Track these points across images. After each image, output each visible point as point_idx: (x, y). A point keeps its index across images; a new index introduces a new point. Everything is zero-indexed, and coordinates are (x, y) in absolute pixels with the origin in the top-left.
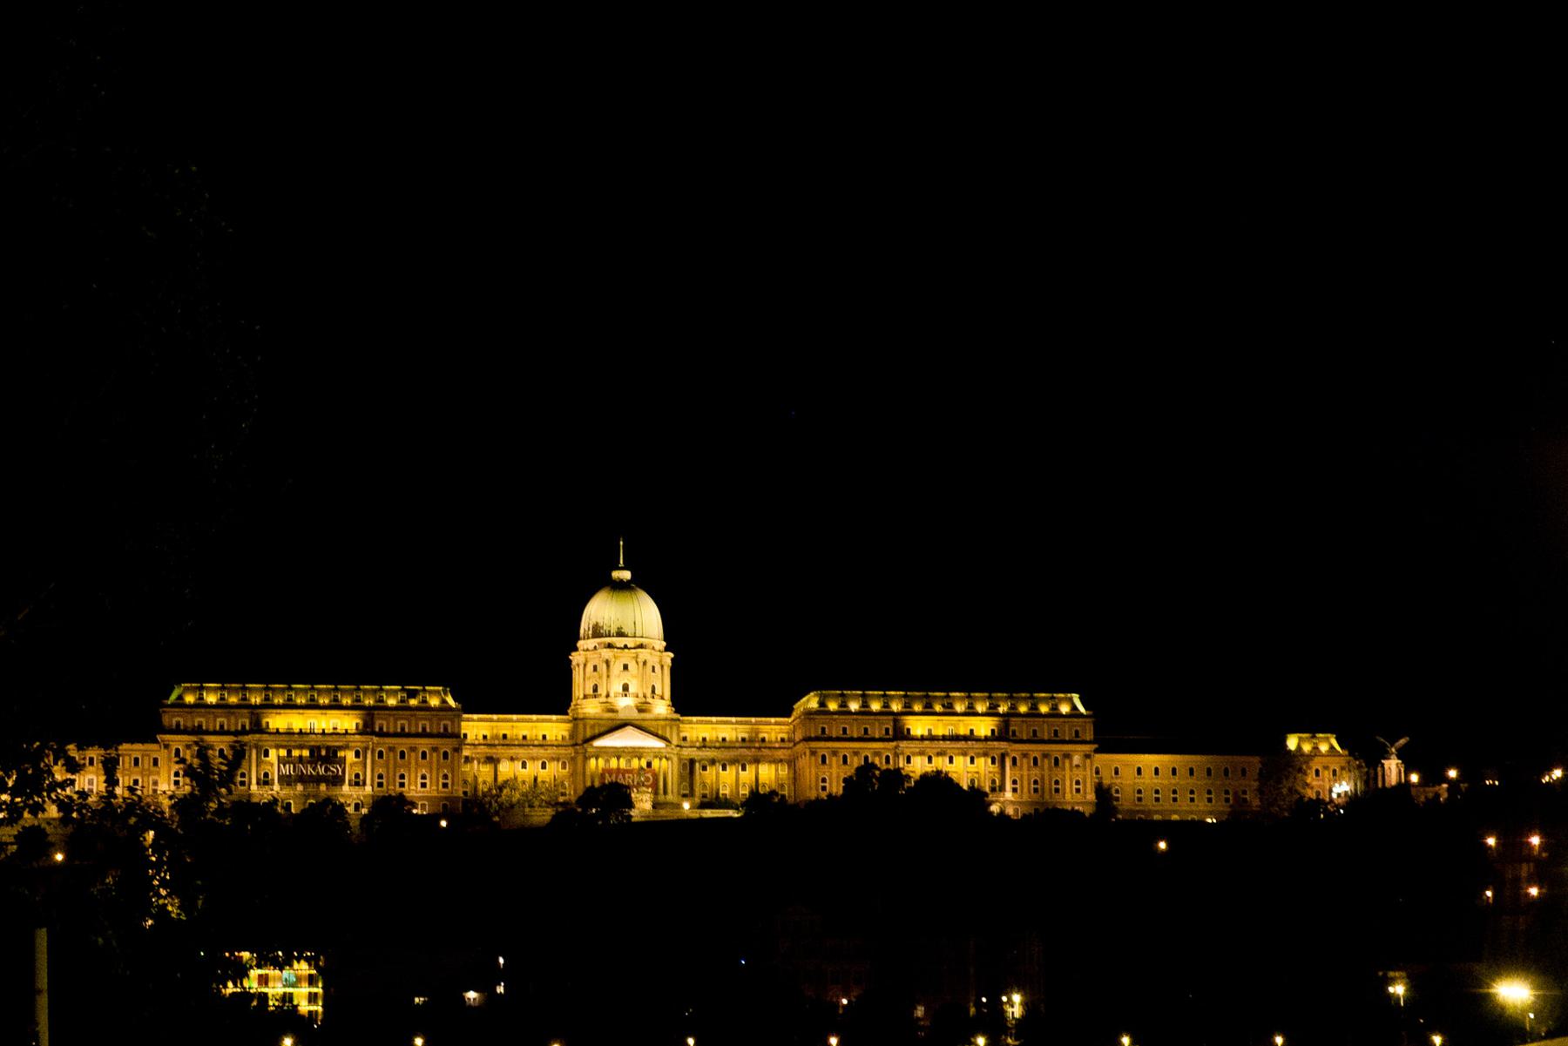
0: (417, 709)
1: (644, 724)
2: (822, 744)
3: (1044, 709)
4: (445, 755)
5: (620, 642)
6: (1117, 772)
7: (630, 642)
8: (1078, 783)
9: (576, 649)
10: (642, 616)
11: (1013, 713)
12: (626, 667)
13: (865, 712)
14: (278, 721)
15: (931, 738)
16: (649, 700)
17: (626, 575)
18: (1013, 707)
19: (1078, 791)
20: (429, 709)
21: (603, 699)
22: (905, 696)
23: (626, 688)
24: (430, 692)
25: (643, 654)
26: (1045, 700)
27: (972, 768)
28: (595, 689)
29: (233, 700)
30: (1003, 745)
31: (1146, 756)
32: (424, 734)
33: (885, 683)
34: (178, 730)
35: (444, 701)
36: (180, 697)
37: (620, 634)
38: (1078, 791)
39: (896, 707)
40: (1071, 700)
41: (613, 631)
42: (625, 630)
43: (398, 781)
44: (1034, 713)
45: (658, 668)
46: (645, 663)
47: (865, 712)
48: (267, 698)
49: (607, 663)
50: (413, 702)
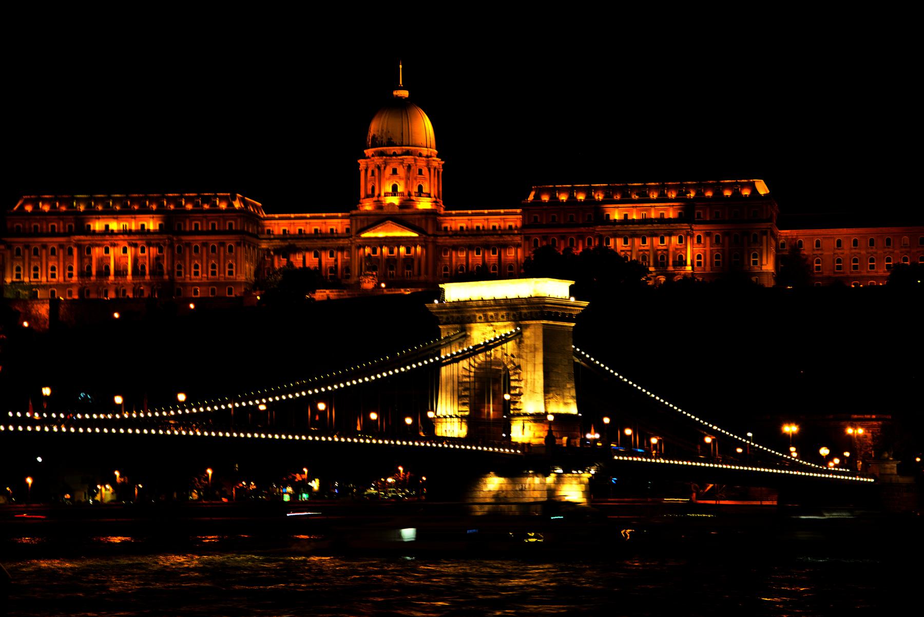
0: (208, 211)
2: (533, 231)
4: (231, 249)
6: (818, 244)
7: (397, 149)
10: (424, 127)
11: (700, 197)
12: (395, 171)
14: (98, 226)
15: (626, 221)
16: (414, 198)
17: (405, 93)
18: (700, 195)
20: (221, 211)
21: (375, 199)
23: (395, 188)
25: (409, 159)
26: (727, 186)
27: (661, 246)
28: (373, 189)
29: (63, 208)
30: (685, 226)
31: (841, 230)
32: (213, 232)
34: (19, 233)
35: (230, 205)
36: (22, 207)
37: (391, 143)
39: (600, 197)
41: (385, 141)
43: (193, 270)
45: (425, 171)
46: (409, 167)
47: (572, 200)
48: (88, 206)
49: (379, 167)
50: (206, 207)
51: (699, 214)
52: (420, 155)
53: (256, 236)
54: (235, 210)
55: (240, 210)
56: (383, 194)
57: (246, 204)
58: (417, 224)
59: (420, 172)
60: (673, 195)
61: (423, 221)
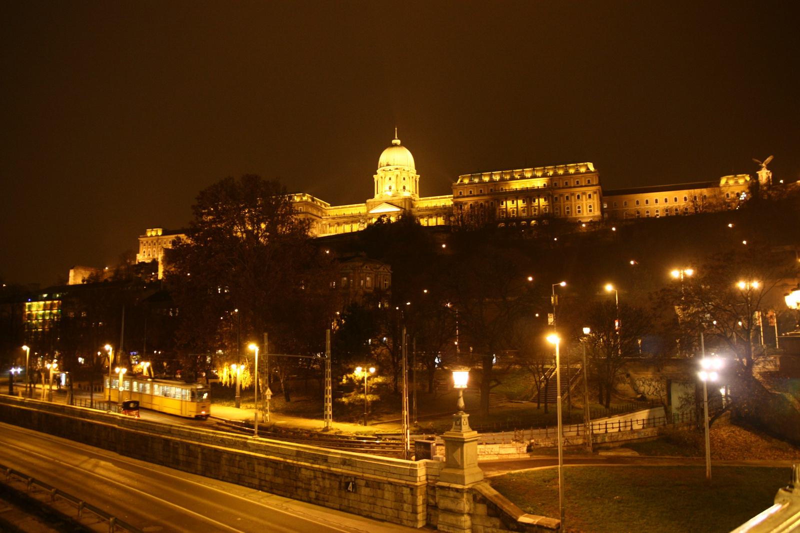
1: (393, 202)
3: (572, 171)
5: (388, 168)
8: (590, 207)
9: (376, 174)
11: (555, 174)
12: (390, 179)
13: (481, 182)
17: (398, 142)
19: (590, 211)
22: (502, 173)
23: (390, 188)
24: (297, 196)
25: (397, 172)
33: (491, 169)
35: (302, 199)
37: (388, 165)
38: (590, 211)
40: (587, 165)
42: (389, 163)
44: (566, 173)
46: (397, 176)
49: (382, 178)
51: (555, 184)
52: (404, 170)
53: (321, 218)
54: (303, 202)
55: (306, 203)
56: (384, 191)
57: (313, 200)
58: (400, 205)
59: (404, 179)
60: (539, 174)
61: (403, 203)
